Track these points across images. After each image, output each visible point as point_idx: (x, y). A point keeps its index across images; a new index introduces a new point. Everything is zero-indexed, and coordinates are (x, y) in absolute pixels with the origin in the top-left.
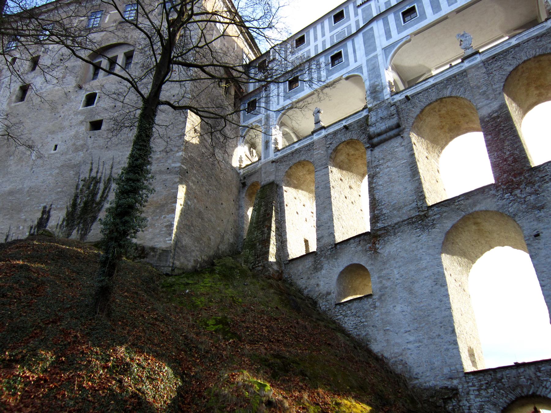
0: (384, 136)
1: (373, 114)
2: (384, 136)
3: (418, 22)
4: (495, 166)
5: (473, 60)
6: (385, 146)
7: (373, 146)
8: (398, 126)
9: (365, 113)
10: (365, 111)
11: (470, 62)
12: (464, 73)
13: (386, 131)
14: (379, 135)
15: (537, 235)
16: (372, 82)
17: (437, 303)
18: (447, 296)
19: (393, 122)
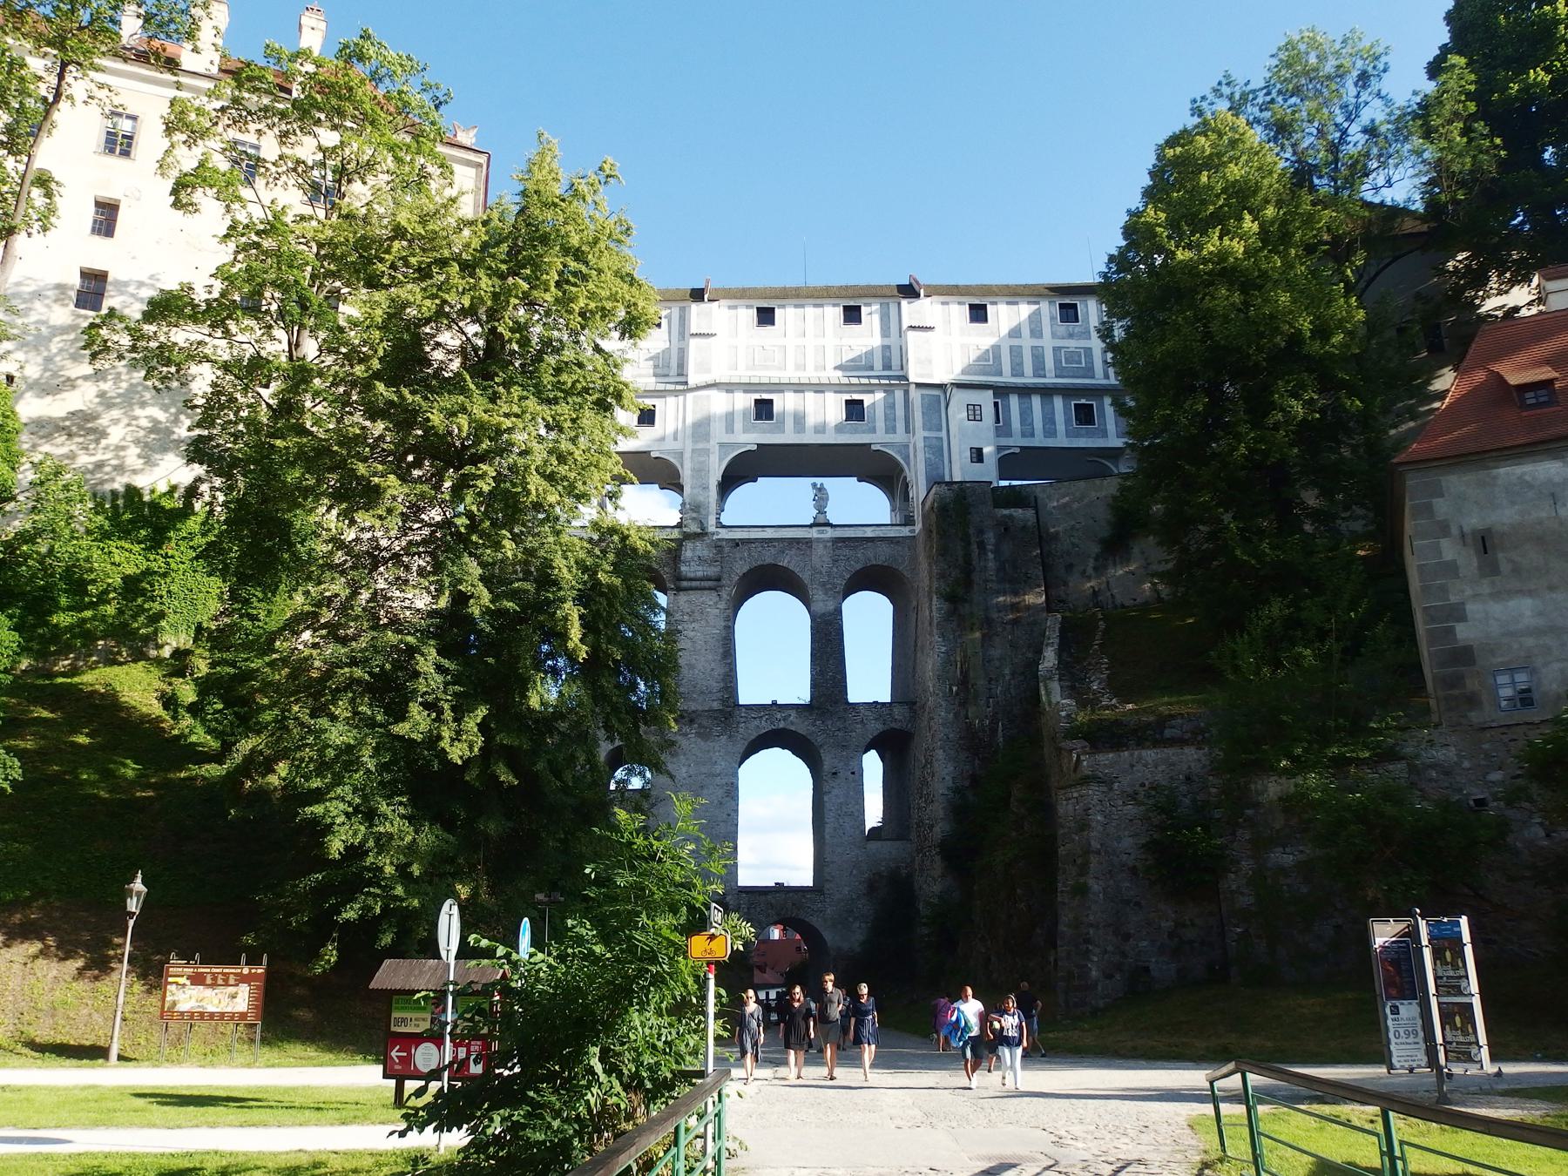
0: (694, 584)
1: (689, 545)
2: (694, 584)
3: (771, 431)
4: (814, 685)
5: (822, 532)
6: (693, 596)
7: (679, 589)
8: (718, 579)
9: (676, 534)
10: (676, 530)
11: (819, 532)
12: (808, 542)
13: (701, 579)
14: (691, 580)
15: (835, 774)
16: (695, 491)
17: (725, 816)
18: (737, 811)
19: (712, 571)
